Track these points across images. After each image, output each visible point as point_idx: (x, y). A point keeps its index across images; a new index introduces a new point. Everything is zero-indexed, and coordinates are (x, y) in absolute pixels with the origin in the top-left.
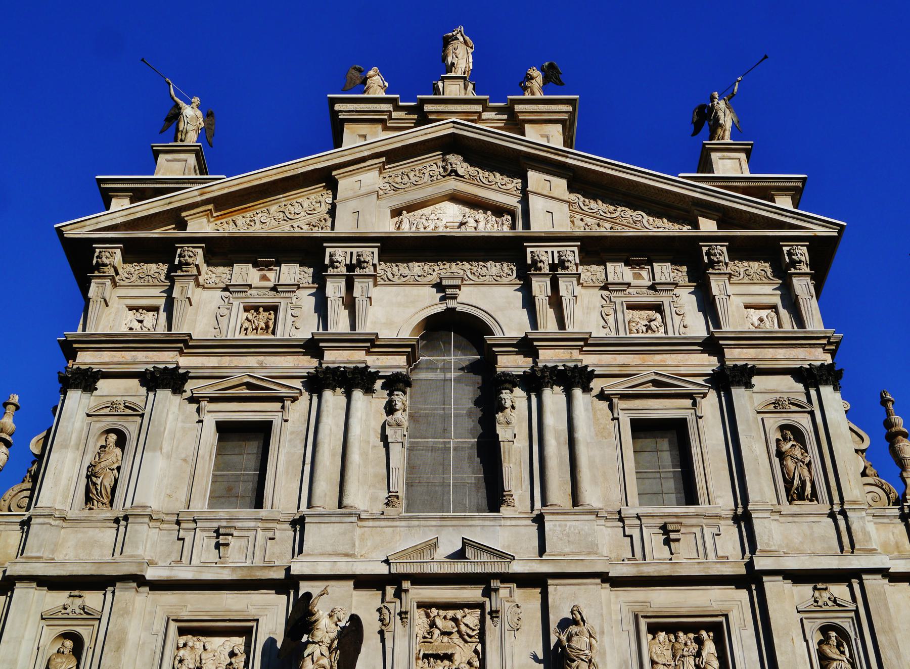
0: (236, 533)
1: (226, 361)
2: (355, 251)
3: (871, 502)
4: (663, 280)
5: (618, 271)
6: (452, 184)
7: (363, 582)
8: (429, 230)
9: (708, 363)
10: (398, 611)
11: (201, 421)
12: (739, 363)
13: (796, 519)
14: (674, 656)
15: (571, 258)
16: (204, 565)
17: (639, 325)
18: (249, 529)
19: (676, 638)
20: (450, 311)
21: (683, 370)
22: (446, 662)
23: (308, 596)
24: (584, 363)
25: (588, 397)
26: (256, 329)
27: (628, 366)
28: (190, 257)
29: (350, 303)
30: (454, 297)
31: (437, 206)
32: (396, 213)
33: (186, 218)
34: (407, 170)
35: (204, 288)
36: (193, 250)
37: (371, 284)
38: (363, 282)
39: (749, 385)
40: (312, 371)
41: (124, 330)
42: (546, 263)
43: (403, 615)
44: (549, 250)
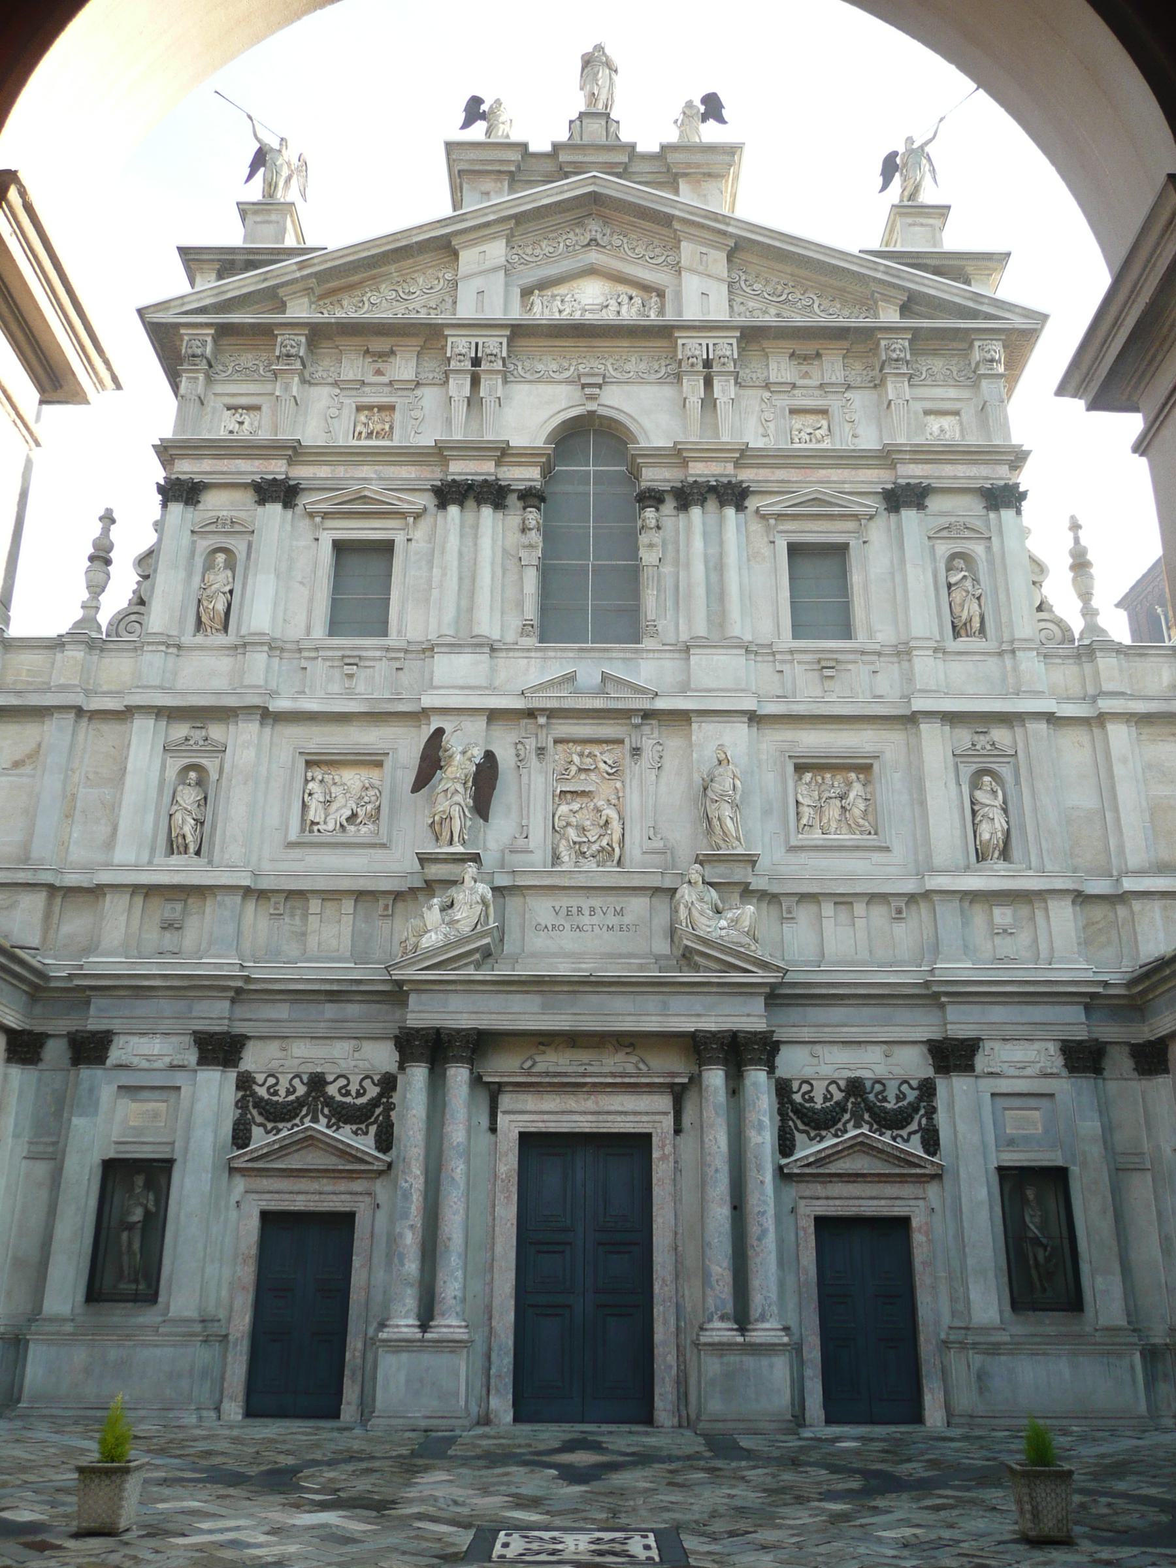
0: (362, 664)
1: (341, 471)
2: (480, 341)
3: (1044, 641)
4: (834, 380)
5: (780, 369)
6: (594, 257)
7: (494, 716)
8: (564, 315)
9: (877, 478)
10: (533, 747)
11: (317, 540)
12: (912, 481)
14: (820, 798)
15: (728, 353)
16: (330, 696)
17: (802, 433)
18: (374, 659)
19: (823, 779)
20: (592, 413)
21: (847, 487)
22: (585, 800)
23: (440, 732)
24: (739, 478)
25: (741, 516)
26: (372, 433)
27: (789, 482)
28: (292, 346)
29: (474, 401)
30: (592, 398)
31: (574, 284)
32: (526, 293)
34: (539, 238)
35: (310, 384)
36: (296, 338)
37: (500, 381)
38: (491, 379)
39: (921, 506)
40: (439, 483)
41: (222, 434)
43: (541, 751)
44: (704, 342)
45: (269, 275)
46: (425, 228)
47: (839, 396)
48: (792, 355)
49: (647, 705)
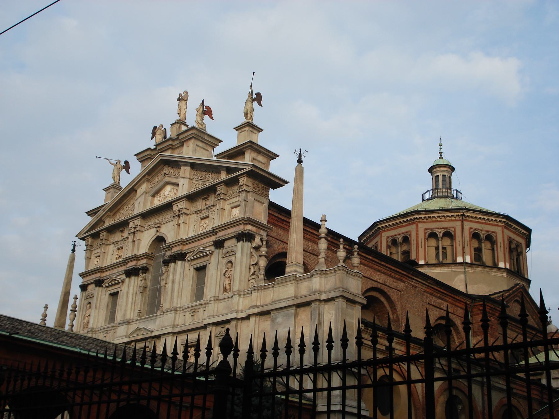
5: (200, 204)
6: (167, 179)
13: (224, 301)
21: (208, 245)
33: (104, 220)
42: (177, 211)
45: (99, 215)
46: (127, 188)
48: (203, 199)
49: (149, 335)
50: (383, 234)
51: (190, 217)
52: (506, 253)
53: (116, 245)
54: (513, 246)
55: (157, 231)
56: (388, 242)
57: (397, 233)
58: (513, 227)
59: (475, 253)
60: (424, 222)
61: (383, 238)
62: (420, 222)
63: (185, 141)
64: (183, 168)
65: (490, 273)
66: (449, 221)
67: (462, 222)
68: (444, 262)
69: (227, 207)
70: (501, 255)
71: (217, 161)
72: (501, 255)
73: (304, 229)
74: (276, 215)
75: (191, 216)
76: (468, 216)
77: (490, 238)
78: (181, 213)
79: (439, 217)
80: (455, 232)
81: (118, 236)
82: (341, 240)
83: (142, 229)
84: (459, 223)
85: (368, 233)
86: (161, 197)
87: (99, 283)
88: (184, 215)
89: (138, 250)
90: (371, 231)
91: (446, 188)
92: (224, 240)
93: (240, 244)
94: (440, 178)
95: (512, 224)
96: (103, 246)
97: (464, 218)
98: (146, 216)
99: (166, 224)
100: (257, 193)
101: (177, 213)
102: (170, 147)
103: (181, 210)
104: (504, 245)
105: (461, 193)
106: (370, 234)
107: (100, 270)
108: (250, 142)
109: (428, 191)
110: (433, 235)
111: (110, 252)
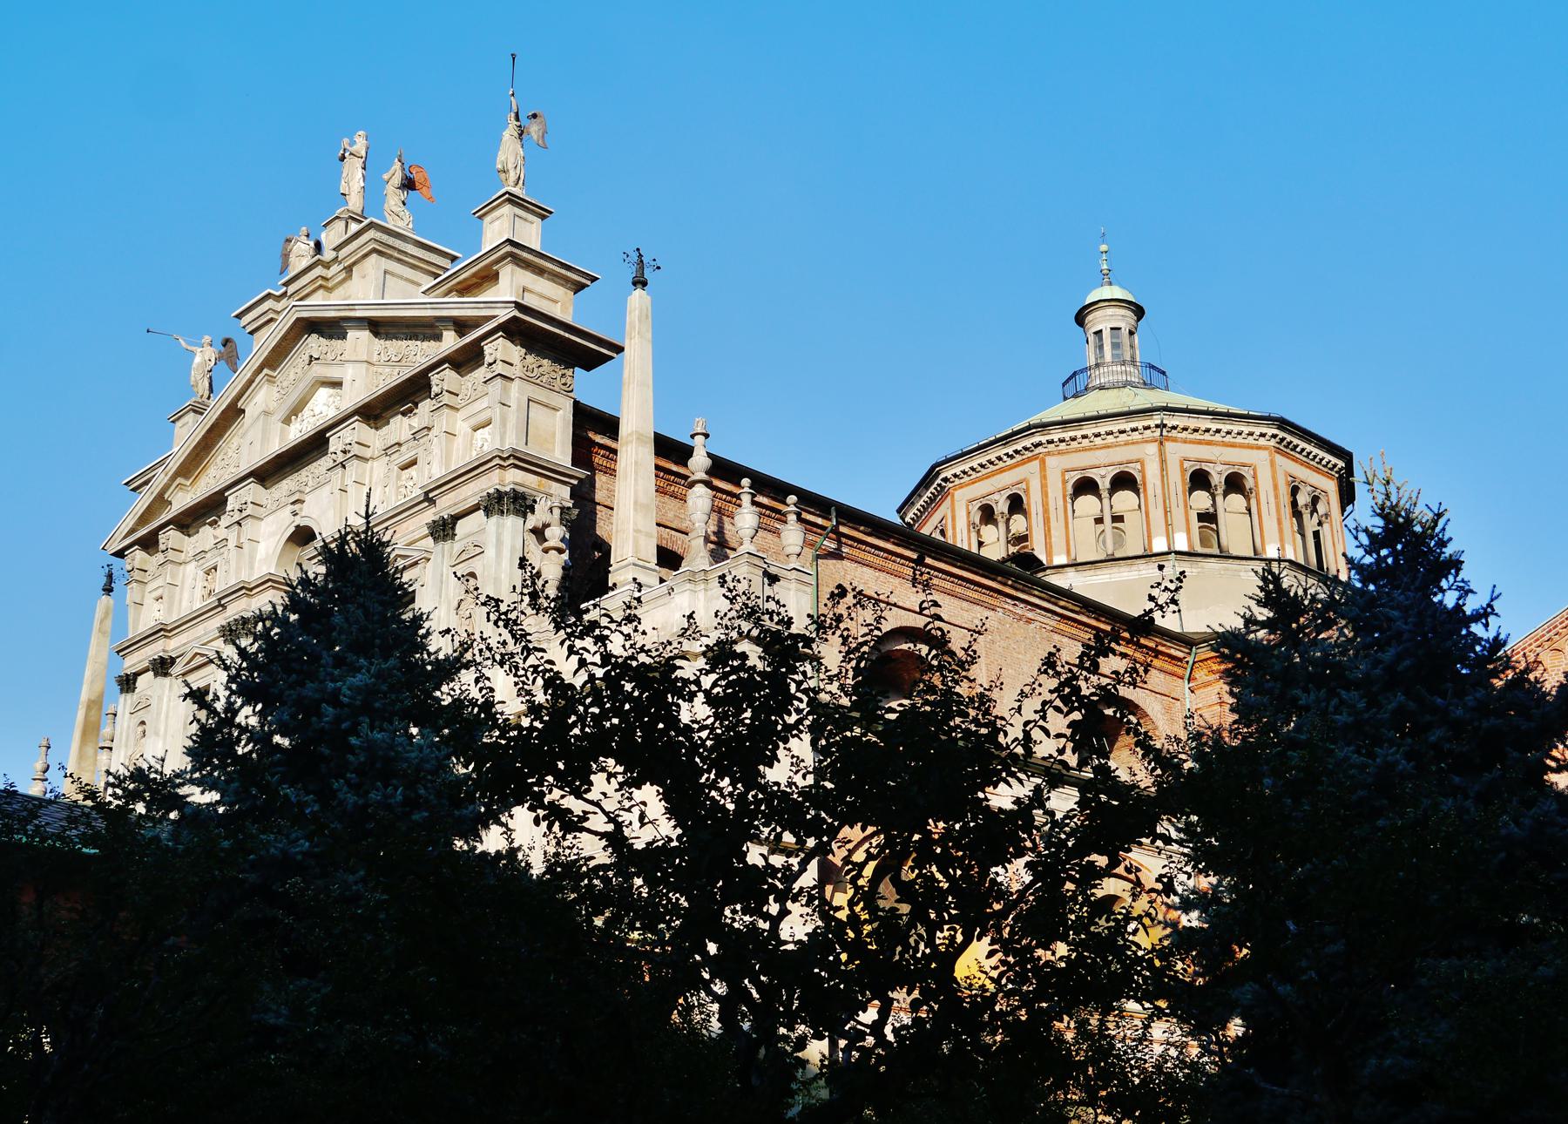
5: (399, 427)
47: (425, 438)
48: (404, 414)
50: (958, 494)
51: (372, 468)
52: (1283, 518)
53: (201, 562)
54: (1303, 499)
55: (295, 514)
56: (972, 514)
57: (992, 489)
58: (1298, 449)
59: (1201, 524)
60: (1060, 453)
61: (957, 504)
62: (1049, 453)
63: (354, 263)
64: (351, 334)
65: (1242, 574)
66: (1127, 444)
67: (1161, 443)
68: (1117, 555)
69: (461, 425)
70: (1270, 524)
71: (428, 306)
72: (1270, 524)
73: (657, 467)
74: (602, 442)
75: (375, 464)
76: (1174, 428)
77: (1235, 483)
78: (349, 455)
79: (1097, 435)
80: (1142, 471)
81: (206, 536)
82: (792, 499)
83: (260, 512)
84: (1152, 449)
85: (920, 496)
86: (306, 421)
87: (162, 666)
88: (355, 462)
89: (252, 568)
90: (927, 490)
91: (1123, 363)
92: (456, 518)
93: (495, 519)
94: (1106, 335)
95: (1296, 441)
96: (169, 566)
97: (1165, 433)
98: (268, 473)
99: (317, 491)
100: (538, 381)
101: (340, 458)
102: (320, 282)
103: (348, 448)
104: (1276, 497)
105: (1164, 373)
106: (925, 498)
107: (162, 631)
108: (509, 242)
109: (1075, 374)
110: (1085, 486)
111: (189, 582)
